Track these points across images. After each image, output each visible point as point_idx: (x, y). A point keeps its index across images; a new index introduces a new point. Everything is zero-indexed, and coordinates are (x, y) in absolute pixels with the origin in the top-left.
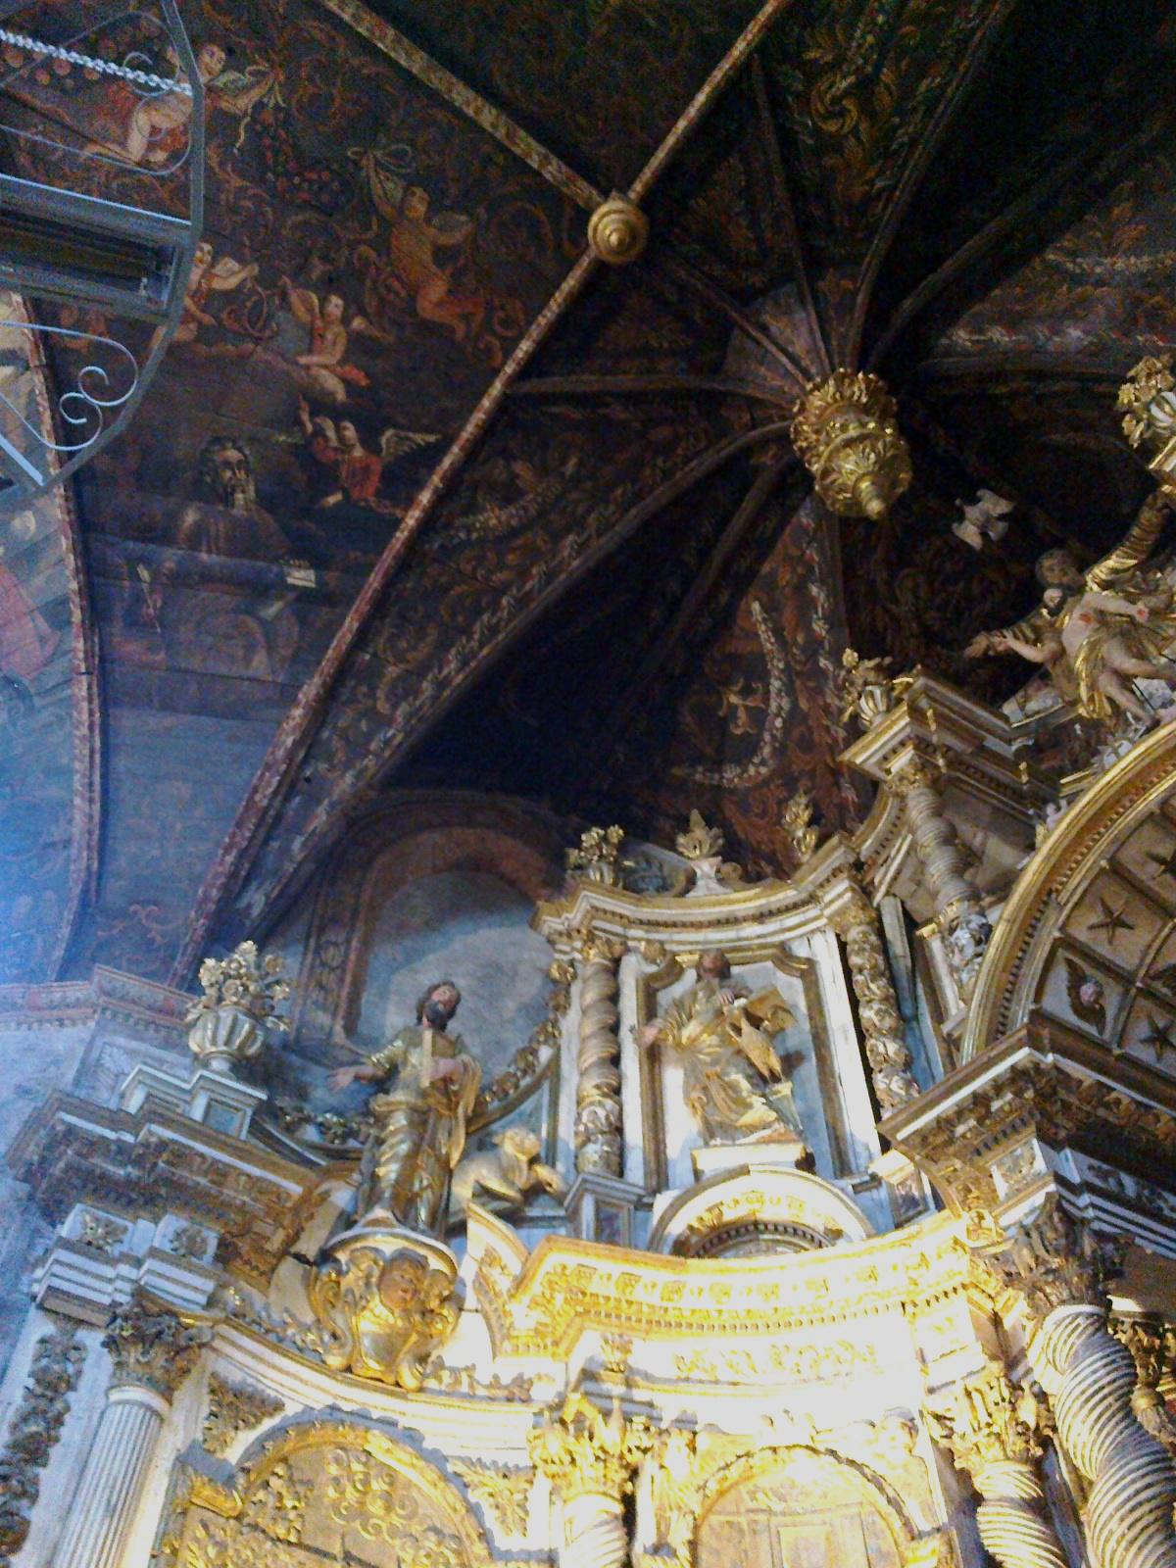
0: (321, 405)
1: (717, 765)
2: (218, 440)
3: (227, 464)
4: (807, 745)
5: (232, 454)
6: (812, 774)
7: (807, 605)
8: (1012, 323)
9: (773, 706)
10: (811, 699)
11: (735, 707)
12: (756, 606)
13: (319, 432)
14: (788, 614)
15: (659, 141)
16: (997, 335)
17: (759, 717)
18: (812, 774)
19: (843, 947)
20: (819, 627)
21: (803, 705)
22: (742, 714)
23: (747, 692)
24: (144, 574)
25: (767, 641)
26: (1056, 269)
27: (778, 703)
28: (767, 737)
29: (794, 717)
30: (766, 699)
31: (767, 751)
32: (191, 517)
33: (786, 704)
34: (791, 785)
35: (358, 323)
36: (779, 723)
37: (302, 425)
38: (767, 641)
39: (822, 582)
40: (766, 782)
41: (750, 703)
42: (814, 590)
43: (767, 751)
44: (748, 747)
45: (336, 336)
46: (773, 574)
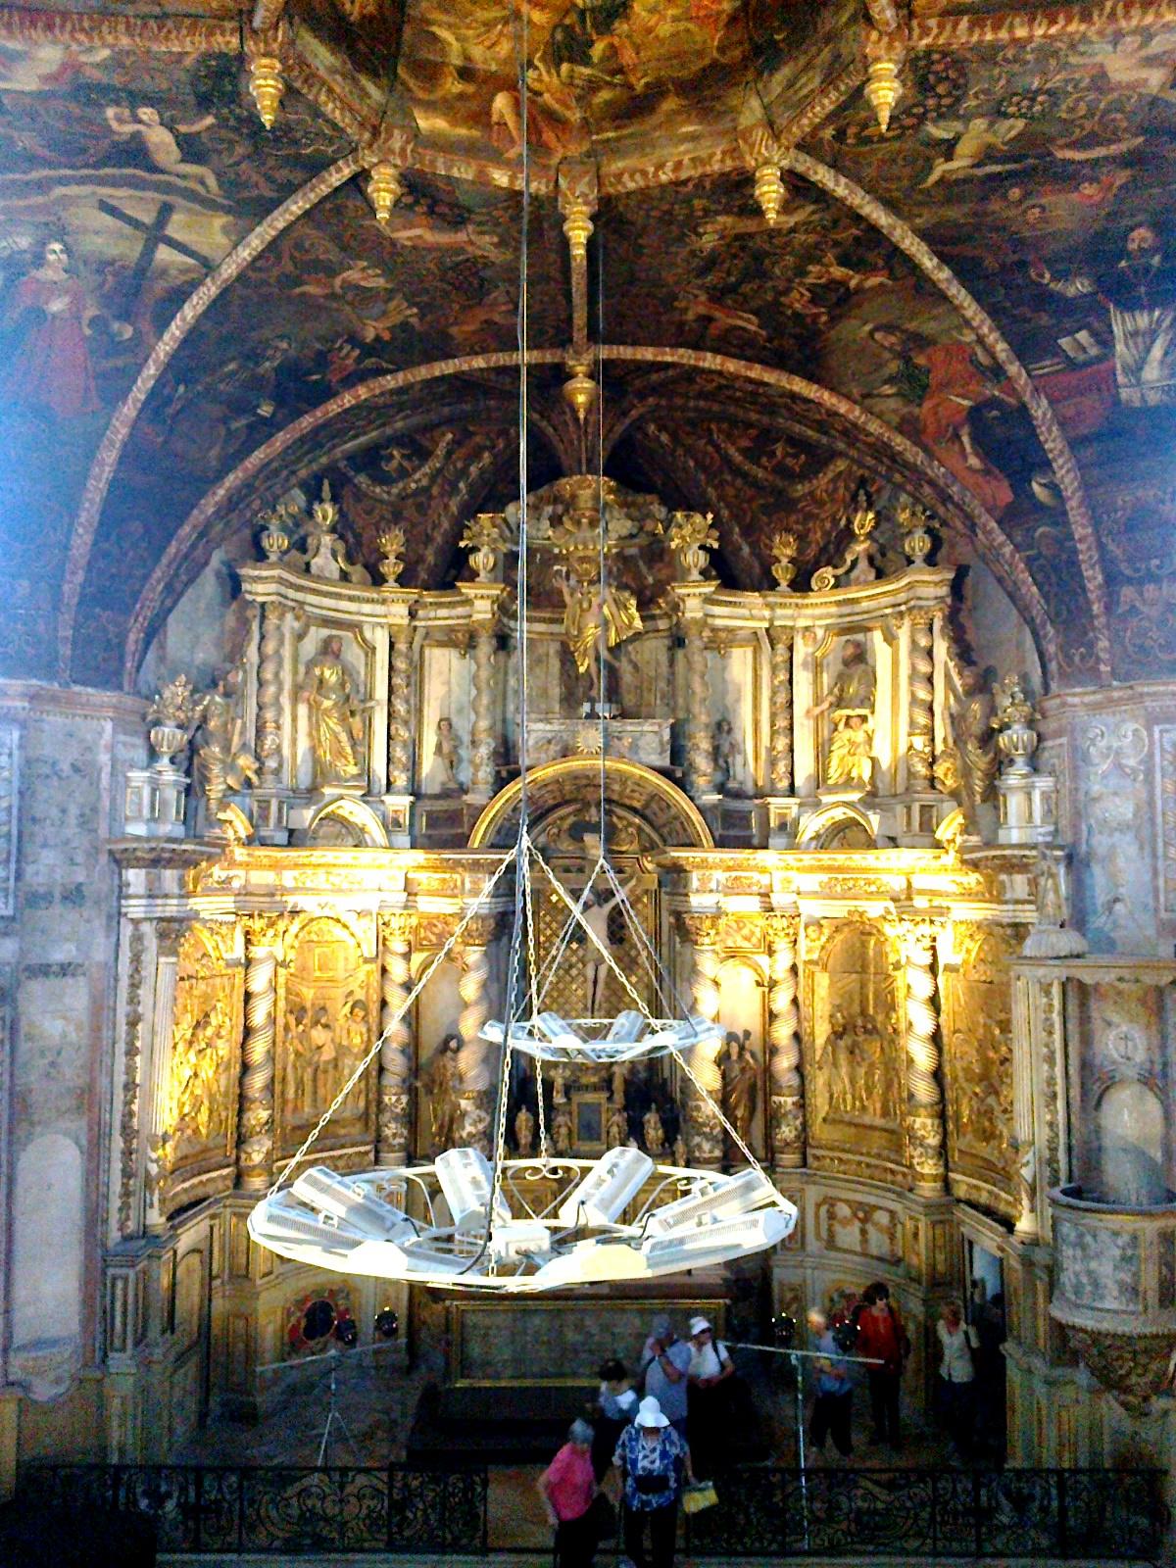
0: (354, 340)
1: (358, 470)
2: (282, 337)
3: (277, 348)
4: (422, 509)
5: (284, 345)
6: (414, 525)
7: (476, 455)
8: (674, 436)
9: (417, 476)
10: (442, 495)
11: (392, 457)
12: (450, 436)
13: (341, 348)
14: (461, 452)
15: (635, 343)
16: (664, 438)
17: (403, 474)
18: (414, 525)
19: (392, 646)
20: (473, 470)
21: (435, 491)
22: (394, 464)
23: (403, 456)
24: (181, 389)
25: (440, 451)
26: (710, 430)
27: (421, 476)
28: (401, 485)
29: (426, 490)
30: (415, 470)
31: (395, 491)
32: (232, 366)
33: (425, 482)
34: (397, 518)
35: (413, 320)
36: (413, 486)
37: (333, 342)
38: (440, 451)
39: (495, 456)
40: (381, 501)
41: (405, 464)
42: (486, 455)
43: (395, 491)
44: (384, 480)
45: (398, 319)
46: (473, 434)
